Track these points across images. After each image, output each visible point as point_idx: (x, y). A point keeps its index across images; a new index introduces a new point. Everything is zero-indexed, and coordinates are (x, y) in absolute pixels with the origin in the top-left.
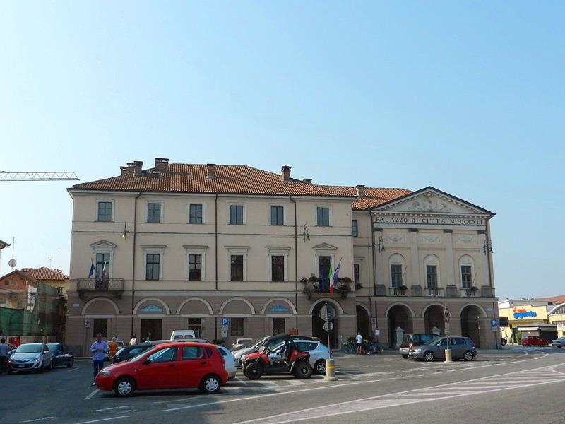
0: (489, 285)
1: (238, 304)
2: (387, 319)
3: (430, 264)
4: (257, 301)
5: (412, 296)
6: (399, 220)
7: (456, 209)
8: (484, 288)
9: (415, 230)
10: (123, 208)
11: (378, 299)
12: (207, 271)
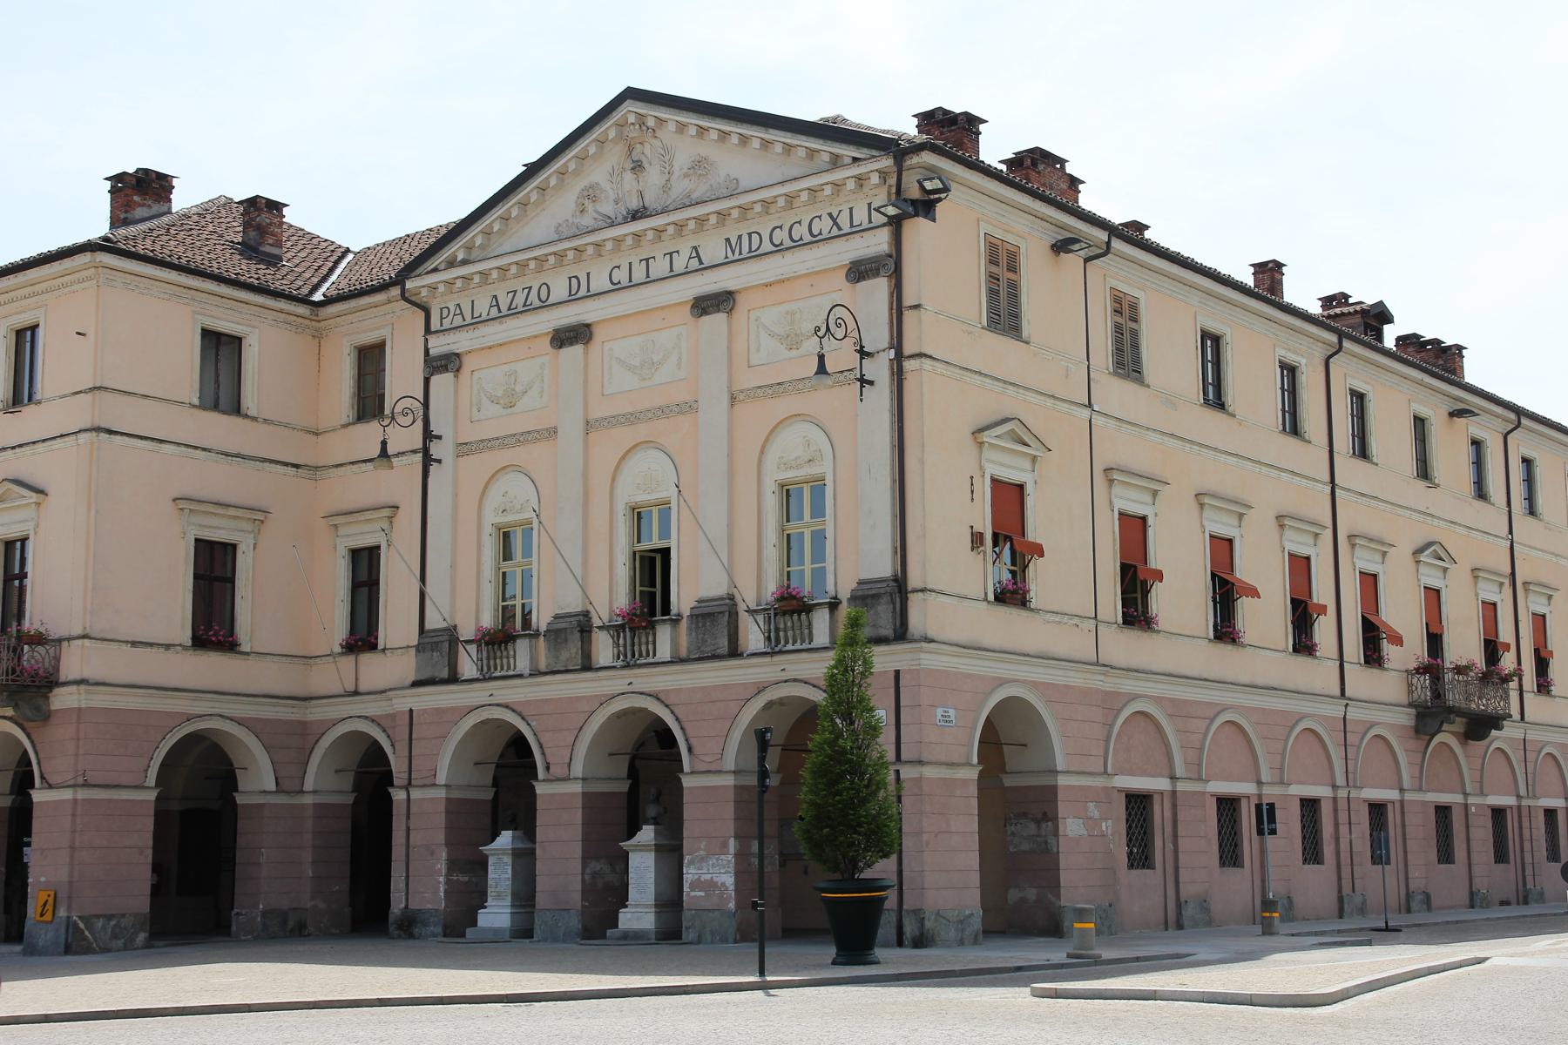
0: (883, 567)
2: (152, 796)
3: (641, 498)
5: (536, 673)
6: (520, 299)
7: (744, 163)
8: (865, 595)
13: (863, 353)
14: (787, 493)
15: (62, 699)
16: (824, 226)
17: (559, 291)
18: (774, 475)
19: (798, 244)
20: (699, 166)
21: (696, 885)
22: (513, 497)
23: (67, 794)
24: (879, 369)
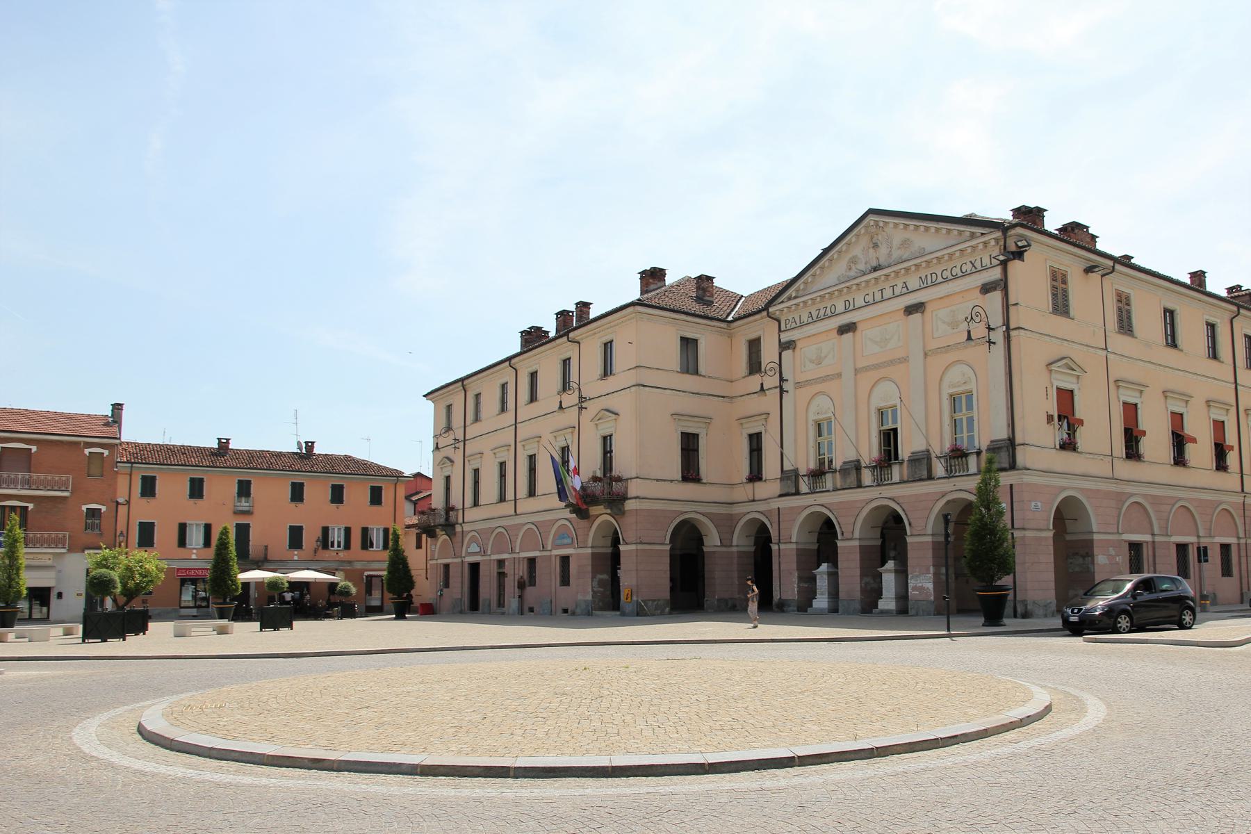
0: (1003, 434)
2: (668, 548)
3: (883, 404)
5: (836, 490)
6: (822, 312)
7: (928, 240)
8: (994, 448)
13: (990, 329)
14: (954, 399)
15: (630, 505)
16: (968, 268)
17: (840, 307)
19: (955, 278)
20: (905, 243)
21: (915, 588)
22: (822, 407)
23: (633, 547)
24: (998, 336)
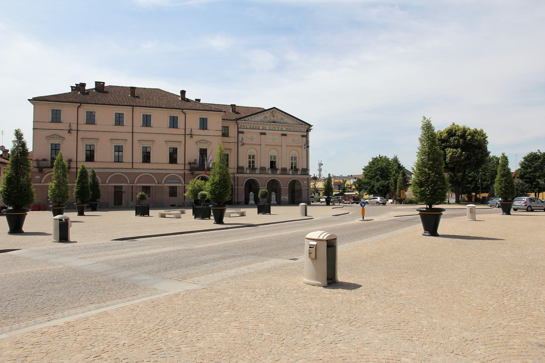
1: (147, 178)
4: (159, 176)
9: (264, 134)
10: (69, 113)
11: (239, 175)
12: (127, 155)
14: (292, 158)
17: (261, 128)
18: (291, 155)
20: (282, 119)
22: (252, 152)
